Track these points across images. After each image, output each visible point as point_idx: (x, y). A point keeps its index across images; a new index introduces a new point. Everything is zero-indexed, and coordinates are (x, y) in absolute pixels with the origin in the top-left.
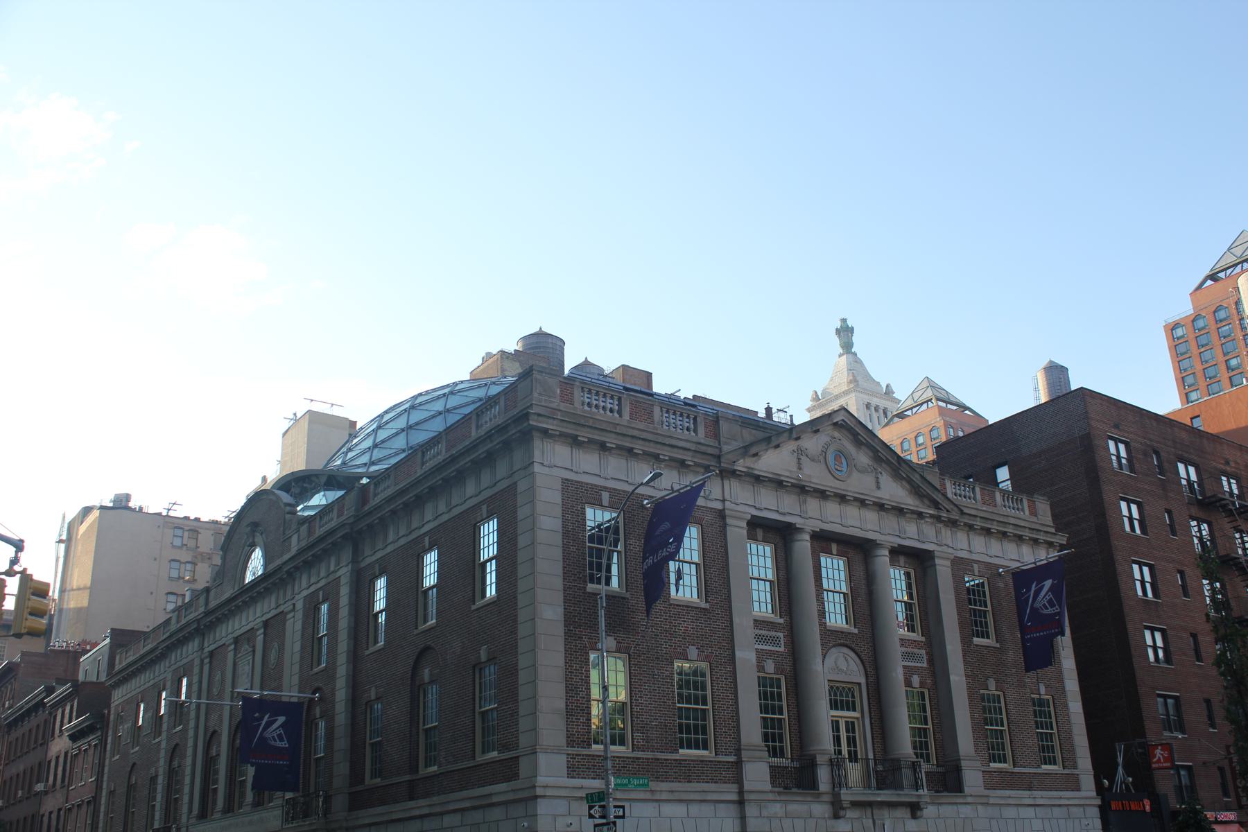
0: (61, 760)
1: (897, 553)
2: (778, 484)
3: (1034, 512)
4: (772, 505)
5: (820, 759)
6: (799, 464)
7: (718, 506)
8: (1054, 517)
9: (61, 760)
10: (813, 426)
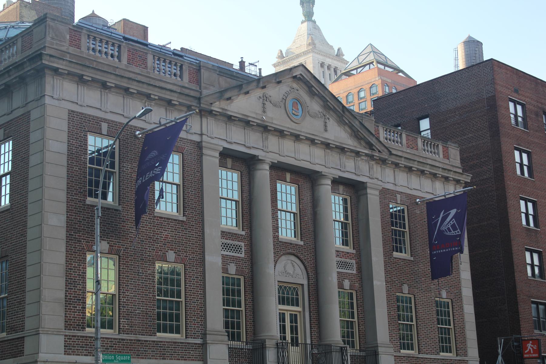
1: (337, 182)
2: (246, 123)
3: (446, 156)
5: (268, 343)
6: (264, 108)
7: (197, 138)
8: (462, 160)
10: (277, 78)
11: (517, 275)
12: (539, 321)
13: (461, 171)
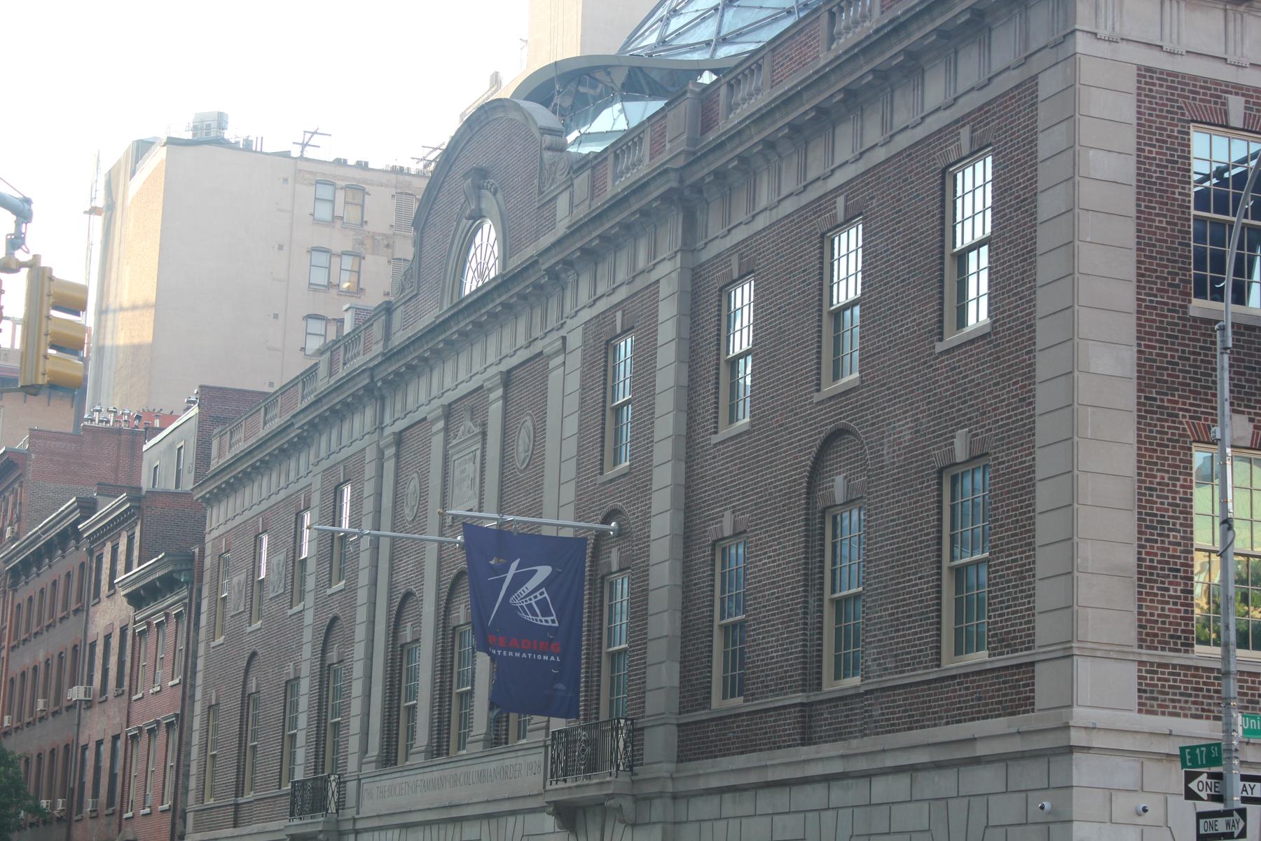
0: (115, 642)
9: (115, 642)
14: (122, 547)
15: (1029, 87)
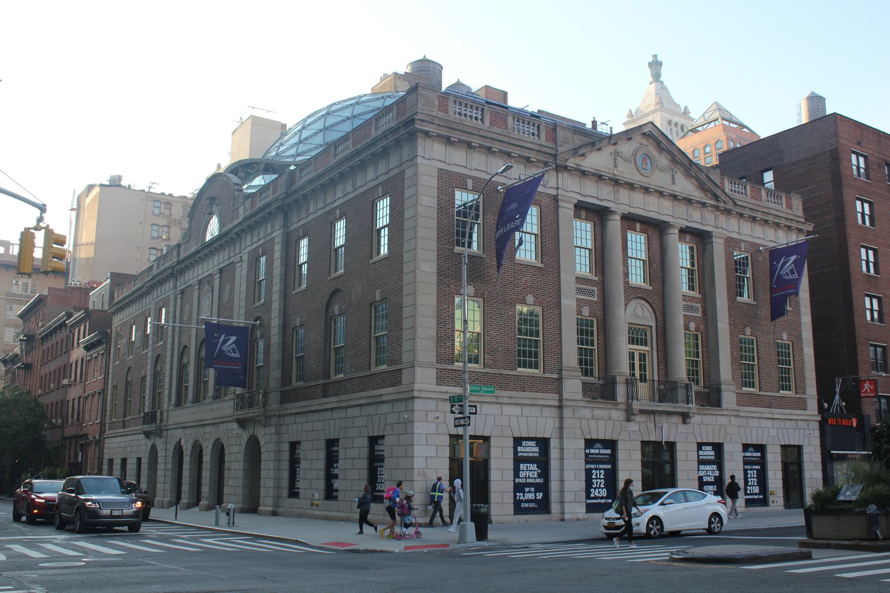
0: (79, 364)
1: (685, 232)
2: (599, 177)
3: (789, 206)
4: (593, 193)
5: (619, 379)
7: (553, 192)
9: (79, 364)
10: (627, 135)
11: (857, 320)
12: (877, 362)
13: (803, 220)
14: (82, 330)
15: (402, 174)
